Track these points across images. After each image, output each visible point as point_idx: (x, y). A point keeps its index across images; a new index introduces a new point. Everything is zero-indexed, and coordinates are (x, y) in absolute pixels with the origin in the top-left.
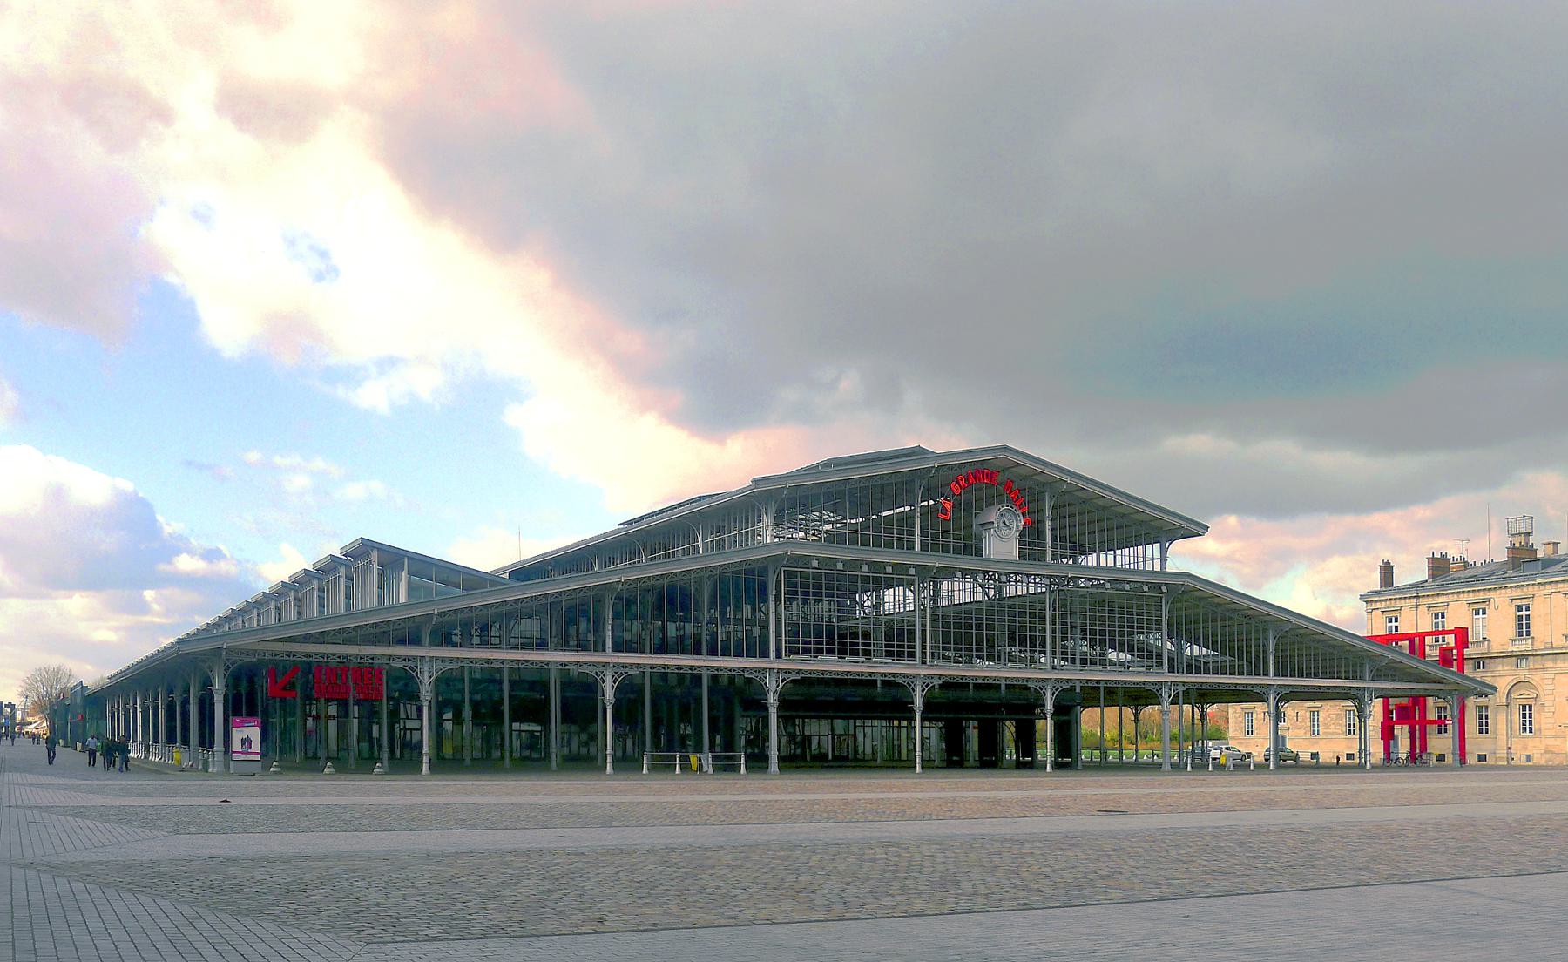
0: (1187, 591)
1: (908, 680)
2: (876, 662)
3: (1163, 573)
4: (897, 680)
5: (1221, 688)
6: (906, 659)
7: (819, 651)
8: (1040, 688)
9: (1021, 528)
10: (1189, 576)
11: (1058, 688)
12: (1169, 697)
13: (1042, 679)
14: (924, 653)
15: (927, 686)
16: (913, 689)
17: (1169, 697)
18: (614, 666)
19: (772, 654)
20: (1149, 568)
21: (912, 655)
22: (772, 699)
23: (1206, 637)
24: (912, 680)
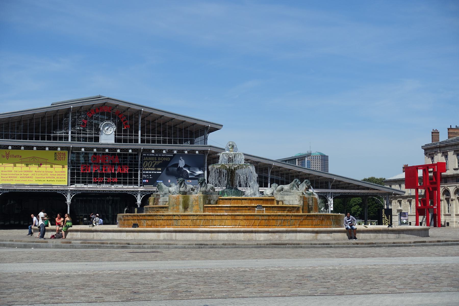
4: (58, 192)
8: (134, 194)
16: (66, 195)
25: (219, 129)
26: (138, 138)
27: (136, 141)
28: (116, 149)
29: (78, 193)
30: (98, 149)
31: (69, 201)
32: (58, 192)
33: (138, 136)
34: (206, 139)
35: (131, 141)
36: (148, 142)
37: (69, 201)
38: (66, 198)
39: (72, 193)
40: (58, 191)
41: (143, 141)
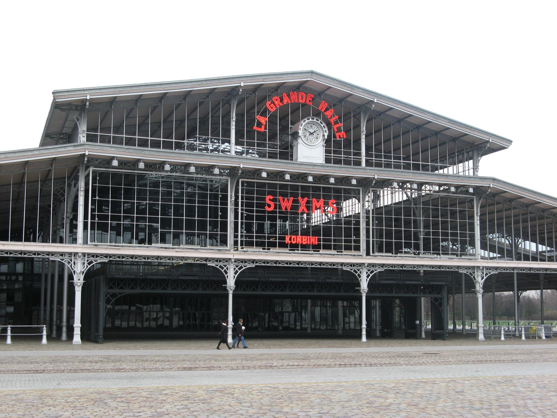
0: (496, 194)
1: (221, 264)
2: (183, 249)
3: (475, 177)
4: (209, 264)
5: (532, 272)
6: (266, 248)
7: (273, 245)
8: (355, 271)
9: (326, 137)
10: (494, 180)
11: (373, 271)
12: (482, 279)
13: (357, 264)
14: (236, 243)
15: (240, 269)
16: (225, 271)
17: (482, 279)
18: (235, 262)
19: (80, 239)
20: (467, 174)
21: (357, 248)
22: (79, 281)
23: (542, 233)
24: (226, 263)
25: (507, 148)
26: (361, 159)
27: (358, 163)
28: (324, 178)
29: (248, 266)
30: (295, 177)
31: (231, 282)
32: (209, 265)
33: (359, 154)
34: (475, 168)
35: (347, 162)
36: (379, 165)
37: (231, 282)
38: (226, 276)
39: (237, 266)
40: (209, 261)
41: (368, 163)
